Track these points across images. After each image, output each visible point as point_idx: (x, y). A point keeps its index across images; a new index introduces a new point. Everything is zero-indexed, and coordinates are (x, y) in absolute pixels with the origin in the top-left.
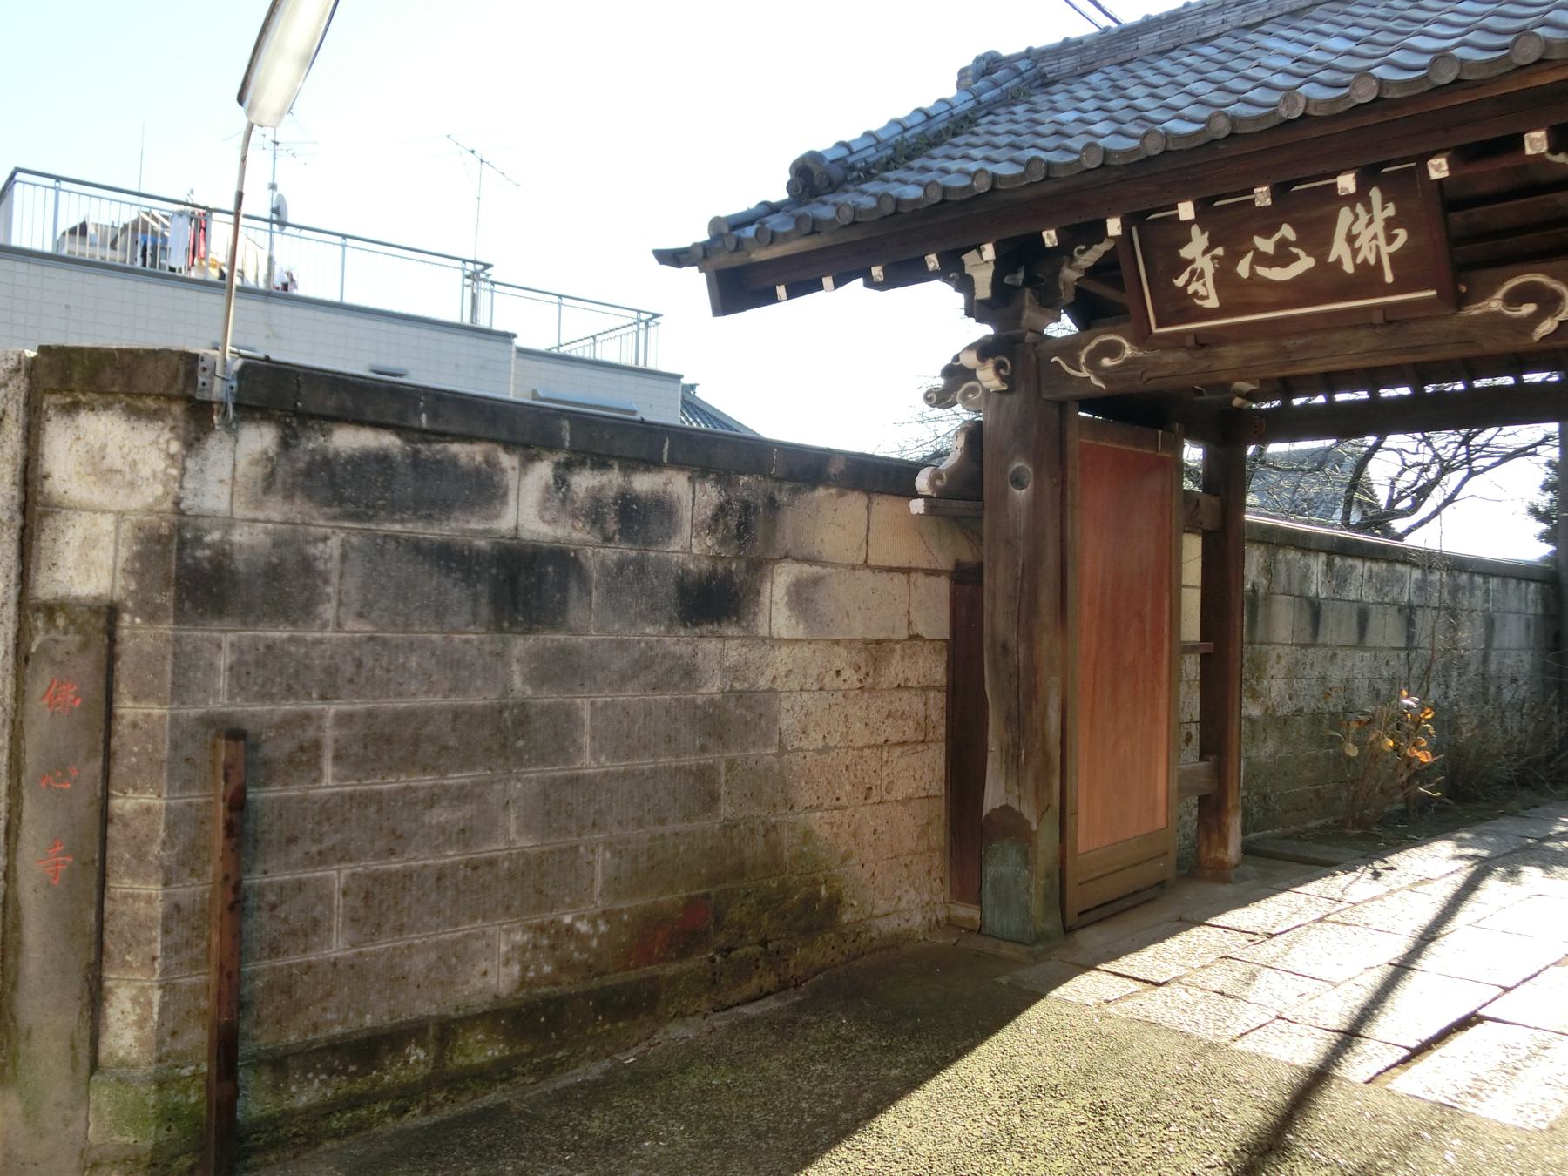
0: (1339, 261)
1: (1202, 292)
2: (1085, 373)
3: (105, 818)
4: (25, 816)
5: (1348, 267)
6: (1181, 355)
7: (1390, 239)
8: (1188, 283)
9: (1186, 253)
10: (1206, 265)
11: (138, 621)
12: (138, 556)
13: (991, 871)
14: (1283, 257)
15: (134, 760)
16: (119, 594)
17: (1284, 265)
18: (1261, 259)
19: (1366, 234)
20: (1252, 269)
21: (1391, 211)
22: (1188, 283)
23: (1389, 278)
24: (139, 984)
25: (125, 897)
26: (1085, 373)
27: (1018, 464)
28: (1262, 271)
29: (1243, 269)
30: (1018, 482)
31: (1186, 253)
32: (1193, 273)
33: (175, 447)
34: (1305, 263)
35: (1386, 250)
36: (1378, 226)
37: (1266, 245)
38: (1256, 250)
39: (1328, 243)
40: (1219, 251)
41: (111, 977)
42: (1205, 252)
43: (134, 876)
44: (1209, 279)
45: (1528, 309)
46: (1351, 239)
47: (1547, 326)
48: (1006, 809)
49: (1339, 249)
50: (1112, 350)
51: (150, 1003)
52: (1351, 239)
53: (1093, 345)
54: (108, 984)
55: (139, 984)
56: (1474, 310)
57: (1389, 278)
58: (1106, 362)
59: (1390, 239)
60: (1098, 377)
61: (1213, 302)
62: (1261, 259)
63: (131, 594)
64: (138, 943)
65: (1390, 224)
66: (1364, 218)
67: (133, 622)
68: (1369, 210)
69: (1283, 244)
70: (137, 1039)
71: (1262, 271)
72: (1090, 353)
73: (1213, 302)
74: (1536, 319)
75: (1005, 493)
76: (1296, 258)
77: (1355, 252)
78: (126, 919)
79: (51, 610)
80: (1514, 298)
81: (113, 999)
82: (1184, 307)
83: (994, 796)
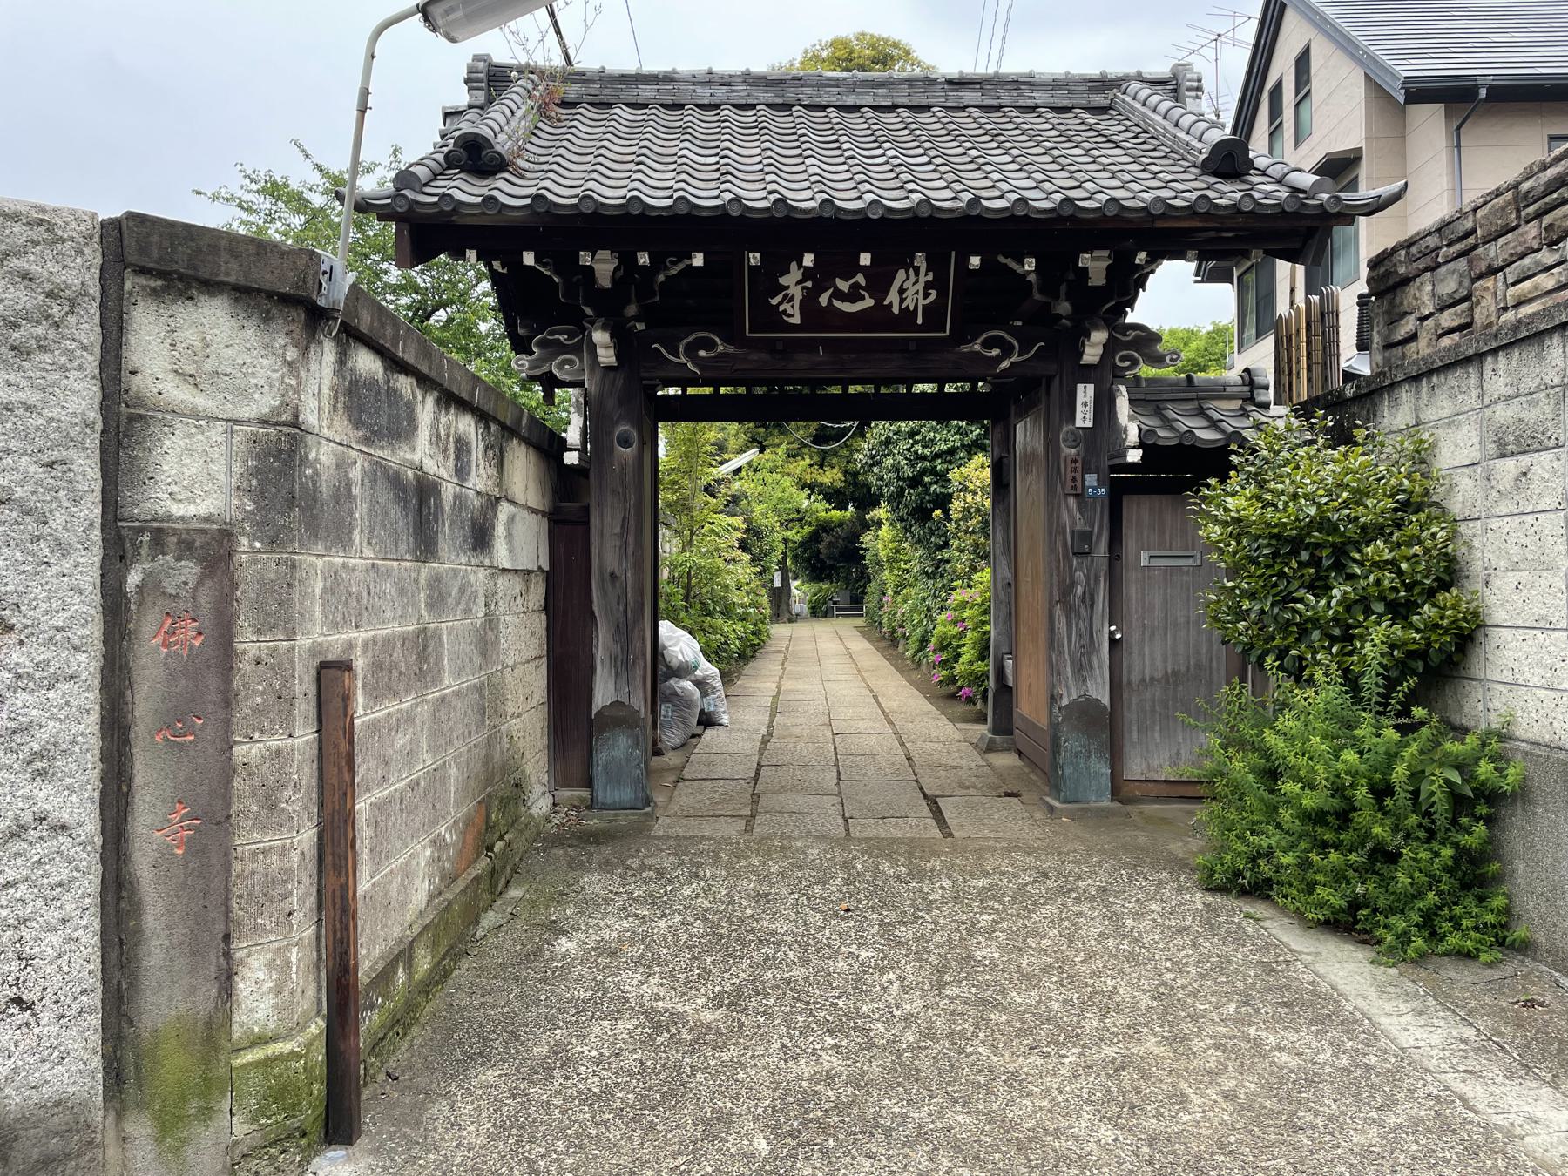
0: (891, 304)
1: (790, 311)
2: (683, 360)
3: (227, 770)
4: (138, 780)
5: (896, 310)
6: (765, 356)
7: (926, 296)
8: (781, 303)
9: (783, 281)
10: (797, 292)
11: (258, 545)
12: (256, 472)
13: (602, 757)
14: (853, 296)
15: (259, 700)
16: (232, 514)
17: (853, 302)
18: (838, 294)
19: (911, 290)
20: (830, 301)
21: (930, 277)
22: (781, 303)
23: (920, 321)
24: (275, 945)
25: (254, 854)
26: (683, 360)
27: (623, 428)
28: (836, 303)
29: (823, 300)
30: (625, 442)
31: (783, 281)
32: (786, 296)
33: (292, 353)
34: (868, 302)
35: (922, 302)
36: (920, 286)
37: (844, 286)
38: (836, 287)
39: (887, 291)
40: (809, 284)
41: (240, 948)
42: (798, 283)
43: (264, 828)
44: (797, 303)
45: (995, 352)
46: (902, 291)
47: (1005, 364)
48: (617, 704)
49: (892, 297)
50: (710, 345)
51: (288, 964)
52: (902, 291)
53: (691, 338)
54: (238, 955)
55: (275, 945)
56: (965, 349)
57: (920, 321)
58: (702, 353)
59: (926, 296)
60: (694, 364)
61: (796, 320)
62: (838, 294)
63: (248, 516)
64: (272, 901)
65: (928, 286)
66: (913, 278)
67: (251, 546)
68: (917, 273)
69: (856, 286)
70: (274, 1007)
71: (836, 303)
72: (688, 345)
73: (796, 320)
74: (999, 359)
75: (611, 450)
76: (863, 298)
77: (902, 300)
78: (256, 878)
79: (160, 535)
80: (988, 344)
81: (244, 971)
82: (775, 319)
83: (604, 692)
